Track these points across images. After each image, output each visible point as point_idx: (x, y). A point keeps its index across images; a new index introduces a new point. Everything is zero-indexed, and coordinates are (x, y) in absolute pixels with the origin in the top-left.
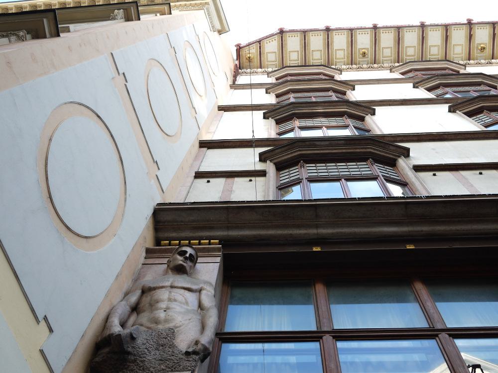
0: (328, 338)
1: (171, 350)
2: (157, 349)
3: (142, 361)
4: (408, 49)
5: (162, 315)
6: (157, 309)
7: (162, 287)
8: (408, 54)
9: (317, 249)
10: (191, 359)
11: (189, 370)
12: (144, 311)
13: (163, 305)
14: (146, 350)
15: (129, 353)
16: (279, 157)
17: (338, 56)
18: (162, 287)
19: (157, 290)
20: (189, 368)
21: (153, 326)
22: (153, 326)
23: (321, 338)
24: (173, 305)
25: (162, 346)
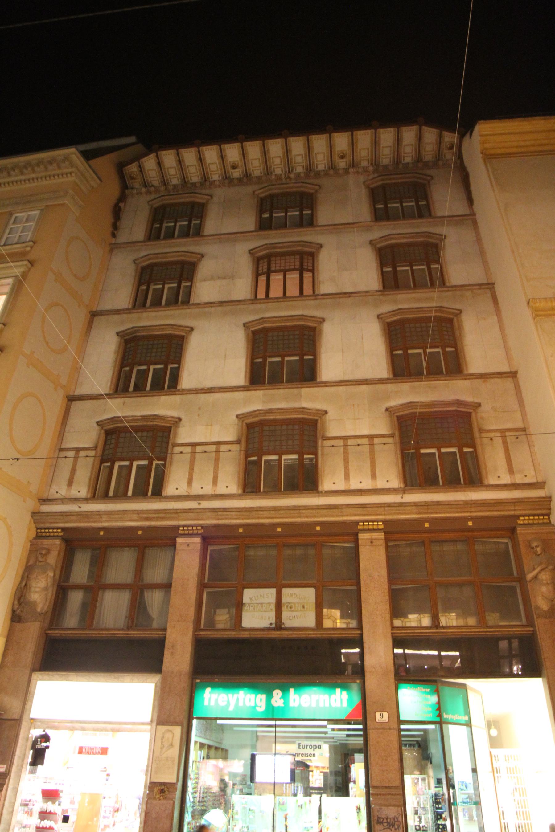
4: (275, 159)
8: (275, 163)
17: (212, 169)
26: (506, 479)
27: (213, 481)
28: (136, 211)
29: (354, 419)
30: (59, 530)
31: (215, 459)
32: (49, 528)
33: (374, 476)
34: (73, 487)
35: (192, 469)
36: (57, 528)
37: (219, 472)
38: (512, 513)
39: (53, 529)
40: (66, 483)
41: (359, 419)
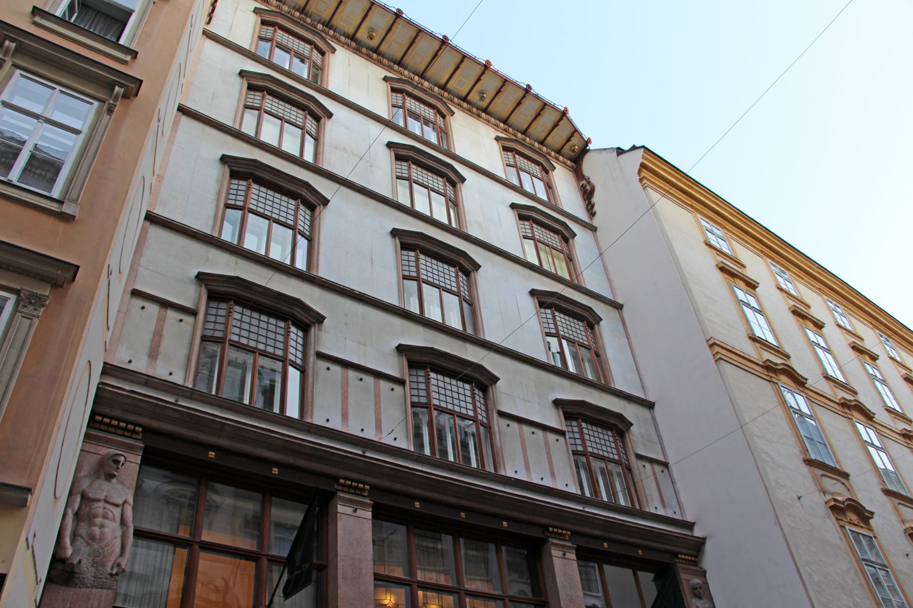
0: (196, 547)
1: (101, 569)
2: (93, 566)
3: (83, 578)
5: (97, 531)
6: (95, 525)
7: (98, 500)
9: (212, 454)
10: (113, 580)
11: (112, 589)
12: (83, 521)
13: (99, 520)
14: (86, 569)
15: (76, 573)
16: (215, 285)
18: (98, 500)
19: (95, 503)
20: (112, 588)
21: (90, 541)
22: (90, 541)
23: (192, 545)
24: (107, 522)
25: (96, 563)
26: (661, 512)
27: (376, 425)
28: (236, 8)
29: (524, 400)
30: (139, 429)
31: (375, 394)
32: (119, 420)
33: (553, 474)
34: (158, 362)
35: (345, 398)
36: (136, 425)
37: (382, 414)
38: (672, 548)
39: (128, 422)
40: (146, 350)
41: (528, 401)
